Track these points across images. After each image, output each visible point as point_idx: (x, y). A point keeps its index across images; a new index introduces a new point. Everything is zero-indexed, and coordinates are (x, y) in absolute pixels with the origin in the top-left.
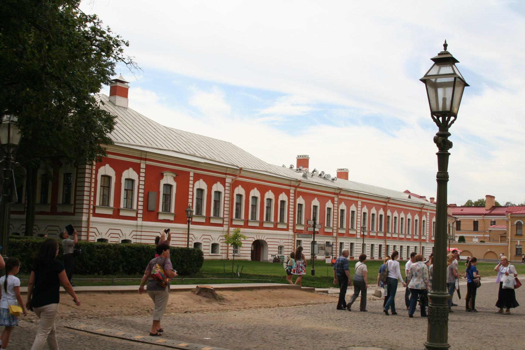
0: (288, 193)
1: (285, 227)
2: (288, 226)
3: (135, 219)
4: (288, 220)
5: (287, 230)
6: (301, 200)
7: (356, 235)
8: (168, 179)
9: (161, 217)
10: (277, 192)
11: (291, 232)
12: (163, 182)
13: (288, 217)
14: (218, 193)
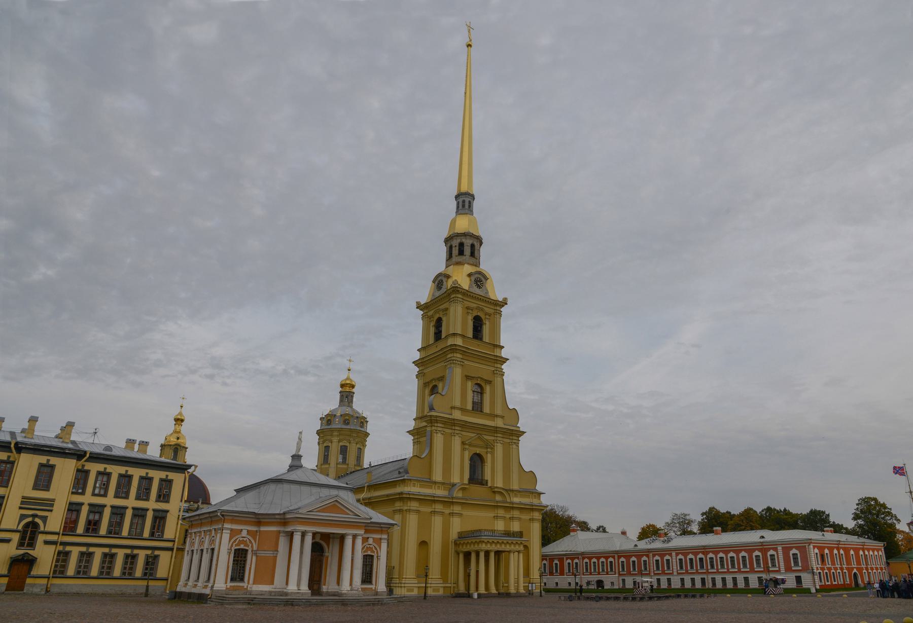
0: (614, 557)
1: (614, 573)
2: (615, 572)
3: (547, 576)
4: (615, 570)
5: (615, 574)
6: (622, 559)
7: (673, 573)
8: (556, 561)
9: (555, 574)
10: (607, 558)
11: (617, 575)
12: (554, 563)
13: (615, 568)
14: (576, 563)
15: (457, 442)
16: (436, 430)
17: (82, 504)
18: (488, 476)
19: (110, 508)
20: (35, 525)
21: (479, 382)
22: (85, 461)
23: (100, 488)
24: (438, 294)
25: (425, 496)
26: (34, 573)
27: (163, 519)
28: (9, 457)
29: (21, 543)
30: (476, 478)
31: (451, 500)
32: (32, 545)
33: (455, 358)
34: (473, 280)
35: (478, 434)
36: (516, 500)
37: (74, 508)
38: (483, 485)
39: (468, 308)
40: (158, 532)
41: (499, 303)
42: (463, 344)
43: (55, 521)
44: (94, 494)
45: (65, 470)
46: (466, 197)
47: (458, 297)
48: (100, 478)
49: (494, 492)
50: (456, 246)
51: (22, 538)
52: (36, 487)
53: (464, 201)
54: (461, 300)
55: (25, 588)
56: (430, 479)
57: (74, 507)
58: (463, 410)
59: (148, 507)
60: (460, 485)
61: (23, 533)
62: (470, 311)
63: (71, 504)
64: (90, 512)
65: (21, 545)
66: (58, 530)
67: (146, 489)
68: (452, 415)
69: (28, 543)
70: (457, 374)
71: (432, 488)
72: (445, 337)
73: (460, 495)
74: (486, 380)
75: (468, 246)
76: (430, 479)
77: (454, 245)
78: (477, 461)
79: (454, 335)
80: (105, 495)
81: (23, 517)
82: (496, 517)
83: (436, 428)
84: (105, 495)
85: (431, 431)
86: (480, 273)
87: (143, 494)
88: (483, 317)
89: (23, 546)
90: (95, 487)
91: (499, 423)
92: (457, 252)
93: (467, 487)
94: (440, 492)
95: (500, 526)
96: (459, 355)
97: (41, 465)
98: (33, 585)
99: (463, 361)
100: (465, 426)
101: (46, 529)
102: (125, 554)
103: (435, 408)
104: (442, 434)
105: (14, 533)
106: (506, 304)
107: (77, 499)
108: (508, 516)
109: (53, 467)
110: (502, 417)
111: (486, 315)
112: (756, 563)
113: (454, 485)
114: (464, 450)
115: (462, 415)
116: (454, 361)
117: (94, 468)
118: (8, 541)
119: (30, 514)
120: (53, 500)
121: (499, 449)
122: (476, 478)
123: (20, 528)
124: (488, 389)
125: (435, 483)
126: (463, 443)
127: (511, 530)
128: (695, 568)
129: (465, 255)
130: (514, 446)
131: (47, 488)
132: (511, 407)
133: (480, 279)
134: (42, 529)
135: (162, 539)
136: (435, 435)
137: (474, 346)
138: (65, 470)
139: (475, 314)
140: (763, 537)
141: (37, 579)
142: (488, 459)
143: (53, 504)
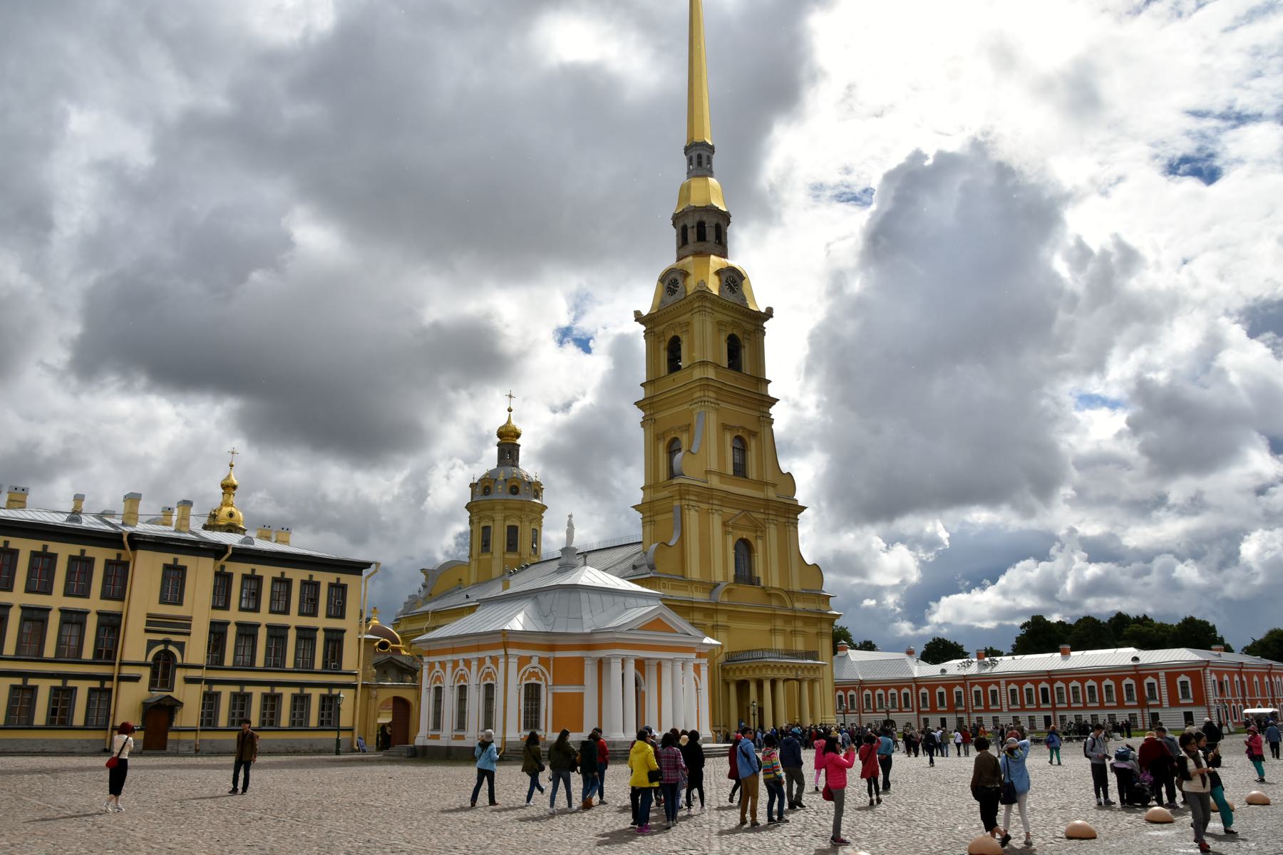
15: (716, 522)
16: (688, 505)
18: (759, 571)
19: (266, 629)
21: (740, 434)
22: (227, 560)
25: (680, 601)
26: (176, 724)
27: (339, 642)
28: (119, 556)
30: (745, 575)
31: (714, 607)
33: (707, 399)
34: (724, 280)
35: (744, 510)
36: (798, 605)
37: (217, 632)
38: (753, 584)
40: (334, 662)
42: (716, 376)
43: (196, 649)
44: (241, 609)
45: (201, 573)
46: (703, 149)
47: (705, 306)
48: (247, 584)
49: (769, 595)
50: (693, 227)
51: (154, 674)
52: (163, 601)
53: (699, 157)
54: (710, 310)
55: (169, 746)
56: (683, 577)
58: (721, 475)
59: (318, 626)
60: (726, 586)
62: (723, 328)
65: (153, 685)
67: (312, 600)
68: (707, 483)
70: (712, 420)
71: (687, 590)
73: (725, 599)
75: (711, 227)
76: (683, 577)
77: (689, 226)
78: (744, 549)
79: (704, 363)
80: (256, 609)
81: (151, 644)
82: (773, 631)
83: (687, 502)
84: (256, 609)
85: (681, 507)
86: (733, 270)
87: (310, 607)
89: (156, 686)
90: (241, 598)
91: (771, 494)
92: (695, 236)
93: (733, 587)
94: (699, 596)
95: (779, 643)
97: (167, 567)
98: (178, 742)
99: (719, 402)
100: (727, 499)
101: (185, 661)
102: (293, 694)
103: (684, 473)
104: (697, 511)
105: (143, 668)
106: (772, 317)
107: (221, 616)
108: (789, 629)
109: (183, 569)
110: (774, 485)
111: (744, 333)
112: (1127, 695)
113: (716, 585)
114: (726, 533)
115: (721, 482)
116: (706, 403)
117: (238, 570)
118: (136, 679)
119: (161, 639)
120: (190, 619)
121: (772, 532)
122: (745, 575)
123: (150, 659)
124: (752, 444)
125: (692, 582)
126: (725, 524)
127: (794, 649)
129: (709, 241)
130: (792, 528)
131: (179, 602)
132: (785, 471)
133: (733, 279)
134: (179, 661)
135: (339, 671)
136: (687, 512)
138: (201, 573)
141: (182, 733)
142: (759, 546)
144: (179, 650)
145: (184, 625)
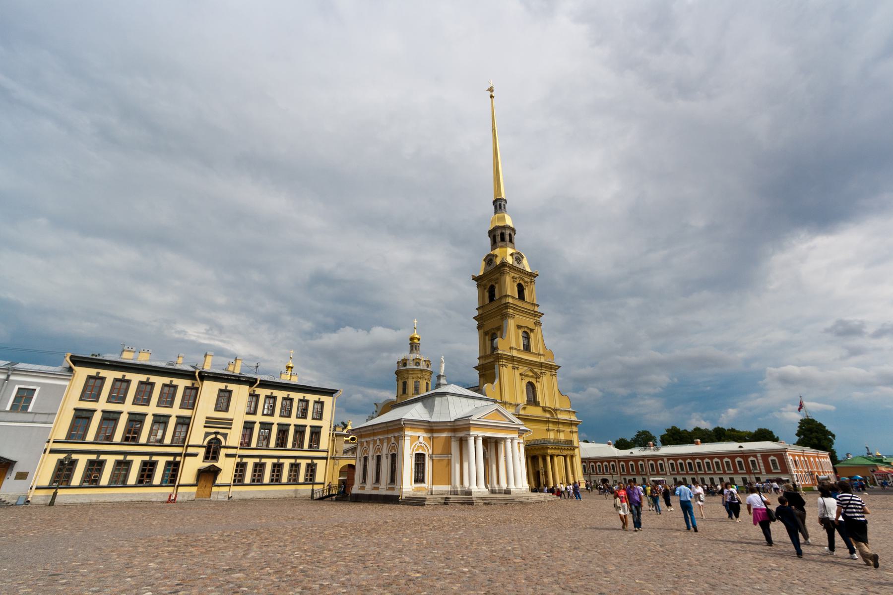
17: (255, 423)
20: (219, 441)
23: (268, 409)
24: (489, 268)
29: (206, 456)
32: (215, 457)
37: (248, 427)
39: (513, 278)
41: (533, 275)
43: (234, 437)
44: (263, 415)
51: (208, 452)
57: (249, 425)
61: (208, 449)
62: (515, 280)
63: (245, 422)
64: (261, 428)
65: (206, 458)
66: (236, 445)
69: (212, 457)
72: (499, 298)
74: (531, 329)
80: (272, 415)
81: (207, 434)
84: (272, 415)
88: (523, 284)
96: (511, 311)
107: (251, 418)
110: (544, 355)
118: (196, 455)
119: (213, 431)
120: (232, 420)
123: (205, 443)
124: (532, 335)
128: (694, 470)
130: (554, 377)
134: (223, 444)
137: (519, 303)
139: (518, 282)
140: (741, 447)
143: (232, 423)
144: (224, 438)
145: (228, 423)
